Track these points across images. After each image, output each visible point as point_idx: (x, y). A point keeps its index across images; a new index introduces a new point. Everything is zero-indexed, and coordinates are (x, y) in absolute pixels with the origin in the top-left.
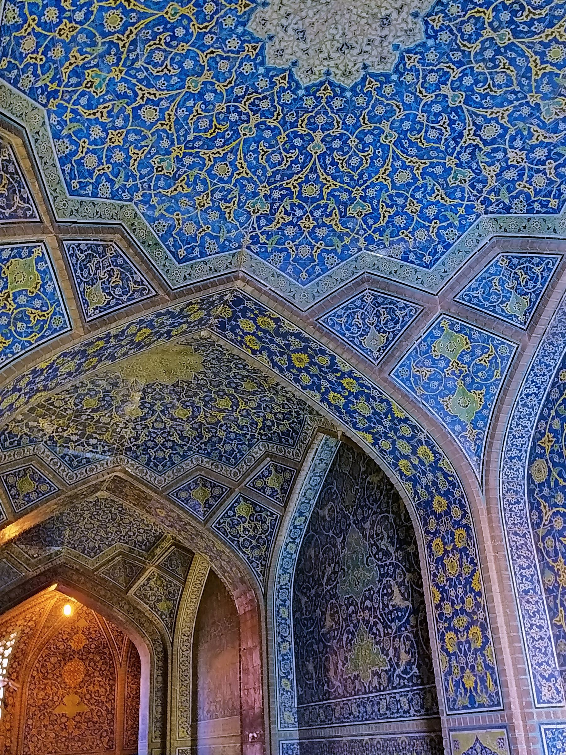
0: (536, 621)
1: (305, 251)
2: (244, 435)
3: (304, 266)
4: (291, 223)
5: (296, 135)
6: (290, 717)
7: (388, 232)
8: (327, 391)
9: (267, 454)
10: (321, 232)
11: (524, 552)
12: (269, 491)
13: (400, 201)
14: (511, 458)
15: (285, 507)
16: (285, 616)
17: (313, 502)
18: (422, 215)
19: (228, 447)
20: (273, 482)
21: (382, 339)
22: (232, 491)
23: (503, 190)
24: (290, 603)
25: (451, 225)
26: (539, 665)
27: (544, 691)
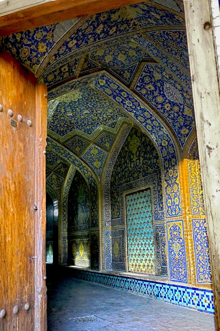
0: (107, 211)
1: (62, 129)
2: (55, 157)
3: (62, 132)
4: (58, 124)
5: (58, 109)
6: (65, 230)
7: (81, 126)
8: (69, 158)
9: (61, 163)
10: (66, 126)
11: (107, 196)
12: (61, 173)
13: (83, 121)
14: (107, 176)
15: (65, 177)
16: (65, 205)
17: (73, 176)
18: (88, 123)
19: (50, 160)
20: (62, 170)
21: (79, 149)
22: (51, 172)
23: (104, 121)
24: (67, 202)
25: (94, 126)
26: (106, 219)
27: (107, 224)
